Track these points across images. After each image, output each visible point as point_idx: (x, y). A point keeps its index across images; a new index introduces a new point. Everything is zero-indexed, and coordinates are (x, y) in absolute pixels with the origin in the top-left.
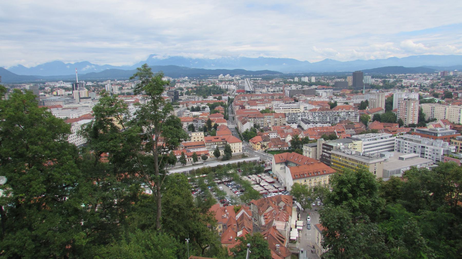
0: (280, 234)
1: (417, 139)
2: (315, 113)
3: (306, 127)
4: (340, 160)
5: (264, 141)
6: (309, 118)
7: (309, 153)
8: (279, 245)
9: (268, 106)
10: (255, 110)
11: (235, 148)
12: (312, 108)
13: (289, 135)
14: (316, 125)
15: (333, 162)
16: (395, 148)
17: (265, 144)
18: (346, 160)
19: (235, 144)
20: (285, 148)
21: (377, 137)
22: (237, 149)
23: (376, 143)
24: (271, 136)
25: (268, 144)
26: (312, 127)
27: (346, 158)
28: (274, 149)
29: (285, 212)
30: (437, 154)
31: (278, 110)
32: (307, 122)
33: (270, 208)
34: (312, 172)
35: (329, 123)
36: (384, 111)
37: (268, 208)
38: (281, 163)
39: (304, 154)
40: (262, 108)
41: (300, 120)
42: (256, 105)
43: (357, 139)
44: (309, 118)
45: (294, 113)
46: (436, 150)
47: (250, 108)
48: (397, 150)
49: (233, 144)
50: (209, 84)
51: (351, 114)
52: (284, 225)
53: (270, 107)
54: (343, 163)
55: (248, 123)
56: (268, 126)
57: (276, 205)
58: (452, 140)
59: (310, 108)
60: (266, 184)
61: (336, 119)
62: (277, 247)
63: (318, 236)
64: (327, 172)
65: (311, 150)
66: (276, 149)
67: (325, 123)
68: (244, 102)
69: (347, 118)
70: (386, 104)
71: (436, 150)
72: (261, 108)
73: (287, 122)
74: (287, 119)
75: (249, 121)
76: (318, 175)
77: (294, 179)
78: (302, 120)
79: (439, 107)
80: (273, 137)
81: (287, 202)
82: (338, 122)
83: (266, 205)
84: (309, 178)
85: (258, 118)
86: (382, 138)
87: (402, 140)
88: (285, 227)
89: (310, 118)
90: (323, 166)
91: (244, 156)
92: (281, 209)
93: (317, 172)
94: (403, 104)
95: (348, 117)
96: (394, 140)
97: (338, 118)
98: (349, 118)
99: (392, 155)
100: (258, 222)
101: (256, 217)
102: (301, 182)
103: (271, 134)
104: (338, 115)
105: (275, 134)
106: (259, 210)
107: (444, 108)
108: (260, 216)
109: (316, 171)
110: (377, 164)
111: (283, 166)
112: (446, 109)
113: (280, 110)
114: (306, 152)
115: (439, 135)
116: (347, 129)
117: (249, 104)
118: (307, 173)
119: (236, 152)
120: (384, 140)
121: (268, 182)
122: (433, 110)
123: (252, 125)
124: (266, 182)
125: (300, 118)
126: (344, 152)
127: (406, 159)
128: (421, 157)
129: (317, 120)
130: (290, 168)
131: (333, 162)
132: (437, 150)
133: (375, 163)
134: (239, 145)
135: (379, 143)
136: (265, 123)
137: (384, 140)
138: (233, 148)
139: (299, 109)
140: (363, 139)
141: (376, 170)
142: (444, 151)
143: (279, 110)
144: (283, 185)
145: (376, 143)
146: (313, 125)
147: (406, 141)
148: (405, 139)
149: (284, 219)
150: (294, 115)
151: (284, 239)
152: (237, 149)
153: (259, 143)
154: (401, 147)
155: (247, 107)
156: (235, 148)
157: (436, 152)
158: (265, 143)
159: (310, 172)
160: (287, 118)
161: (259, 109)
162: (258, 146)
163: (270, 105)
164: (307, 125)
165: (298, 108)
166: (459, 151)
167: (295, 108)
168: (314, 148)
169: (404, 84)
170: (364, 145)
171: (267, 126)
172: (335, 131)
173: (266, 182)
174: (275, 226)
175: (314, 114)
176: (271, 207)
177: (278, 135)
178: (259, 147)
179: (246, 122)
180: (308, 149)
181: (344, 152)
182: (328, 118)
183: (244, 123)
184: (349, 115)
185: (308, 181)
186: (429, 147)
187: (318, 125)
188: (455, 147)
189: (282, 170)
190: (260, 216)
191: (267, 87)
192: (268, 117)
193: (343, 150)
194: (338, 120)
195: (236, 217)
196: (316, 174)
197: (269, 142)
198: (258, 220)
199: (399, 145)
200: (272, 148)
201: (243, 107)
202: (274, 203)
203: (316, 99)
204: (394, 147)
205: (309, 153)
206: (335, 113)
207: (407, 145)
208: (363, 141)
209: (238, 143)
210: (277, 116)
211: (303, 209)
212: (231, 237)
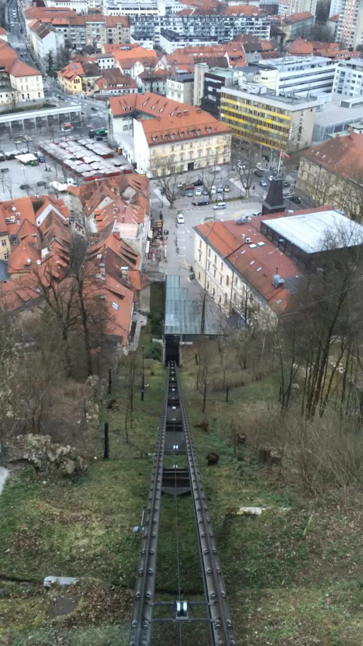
0: (128, 246)
2: (188, 17)
3: (169, 46)
4: (237, 107)
5: (89, 74)
6: (175, 29)
7: (179, 96)
8: (126, 268)
9: (94, 6)
10: (68, 10)
11: (27, 88)
12: (181, 9)
13: (138, 63)
14: (190, 43)
15: (224, 112)
16: (334, 87)
17: (91, 80)
18: (248, 107)
19: (26, 80)
21: (304, 63)
22: (33, 91)
23: (302, 76)
24: (101, 64)
25: (96, 81)
26: (183, 47)
27: (248, 102)
28: (110, 91)
29: (135, 206)
32: (173, 37)
33: (107, 201)
34: (185, 130)
35: (215, 39)
36: (314, 20)
37: (101, 200)
38: (124, 116)
39: (169, 96)
41: (157, 33)
43: (269, 68)
44: (175, 29)
45: (146, 17)
48: (337, 89)
49: (24, 79)
51: (256, 22)
52: (136, 229)
53: (98, 9)
54: (243, 114)
55: (52, 34)
56: (95, 44)
57: (118, 194)
59: (179, 10)
60: (97, 158)
61: (227, 33)
62: (124, 272)
63: (201, 247)
64: (214, 131)
65: (182, 89)
66: (114, 91)
67: (206, 40)
73: (133, 36)
74: (132, 30)
75: (55, 31)
76: (196, 137)
77: (150, 145)
78: (164, 33)
80: (106, 67)
81: (140, 188)
82: (231, 39)
83: (97, 194)
84: (180, 143)
85: (73, 26)
86: (313, 66)
88: (138, 233)
89: (180, 30)
90: (206, 118)
91: (47, 106)
92: (128, 202)
93: (194, 131)
95: (251, 28)
96: (333, 70)
97: (232, 30)
98: (252, 30)
99: (330, 99)
100: (84, 229)
101: (79, 220)
102: (165, 151)
103: (101, 60)
104: (232, 25)
105: (110, 59)
106: (84, 204)
108: (88, 216)
109: (192, 128)
110: (305, 112)
111: (127, 122)
114: (173, 94)
116: (247, 52)
118: (176, 133)
119: (31, 99)
120: (317, 69)
121: (100, 155)
123: (62, 40)
124: (97, 154)
125: (158, 29)
126: (245, 90)
127: (353, 105)
129: (192, 34)
130: (143, 121)
131: (224, 112)
134: (35, 82)
135: (307, 75)
137: (317, 69)
138: (25, 88)
139: (155, 12)
140: (279, 67)
141: (303, 126)
144: (129, 160)
145: (302, 76)
146: (185, 43)
147: (354, 72)
148: (354, 67)
149: (135, 219)
150: (146, 21)
151: (136, 256)
152: (33, 91)
153: (78, 78)
154: (345, 83)
156: (27, 88)
158: (91, 78)
159: (182, 130)
160: (132, 27)
161: (75, 10)
162: (76, 85)
164: (173, 43)
167: (148, 9)
168: (188, 84)
170: (281, 80)
172: (226, 55)
173: (97, 154)
174: (118, 233)
175: (186, 20)
176: (107, 198)
178: (79, 86)
179: (49, 32)
180: (176, 88)
181: (245, 90)
182: (213, 30)
183: (42, 34)
184: (252, 24)
185: (177, 149)
187: (195, 43)
189: (127, 132)
190: (88, 216)
192: (93, 25)
194: (232, 34)
195: (38, 220)
196: (194, 134)
197: (97, 77)
198: (84, 225)
199: (342, 81)
200: (105, 90)
202: (113, 190)
204: (331, 85)
205: (179, 96)
206: (226, 20)
207: (357, 79)
208: (280, 71)
209: (34, 78)
211: (169, 204)
212: (29, 261)
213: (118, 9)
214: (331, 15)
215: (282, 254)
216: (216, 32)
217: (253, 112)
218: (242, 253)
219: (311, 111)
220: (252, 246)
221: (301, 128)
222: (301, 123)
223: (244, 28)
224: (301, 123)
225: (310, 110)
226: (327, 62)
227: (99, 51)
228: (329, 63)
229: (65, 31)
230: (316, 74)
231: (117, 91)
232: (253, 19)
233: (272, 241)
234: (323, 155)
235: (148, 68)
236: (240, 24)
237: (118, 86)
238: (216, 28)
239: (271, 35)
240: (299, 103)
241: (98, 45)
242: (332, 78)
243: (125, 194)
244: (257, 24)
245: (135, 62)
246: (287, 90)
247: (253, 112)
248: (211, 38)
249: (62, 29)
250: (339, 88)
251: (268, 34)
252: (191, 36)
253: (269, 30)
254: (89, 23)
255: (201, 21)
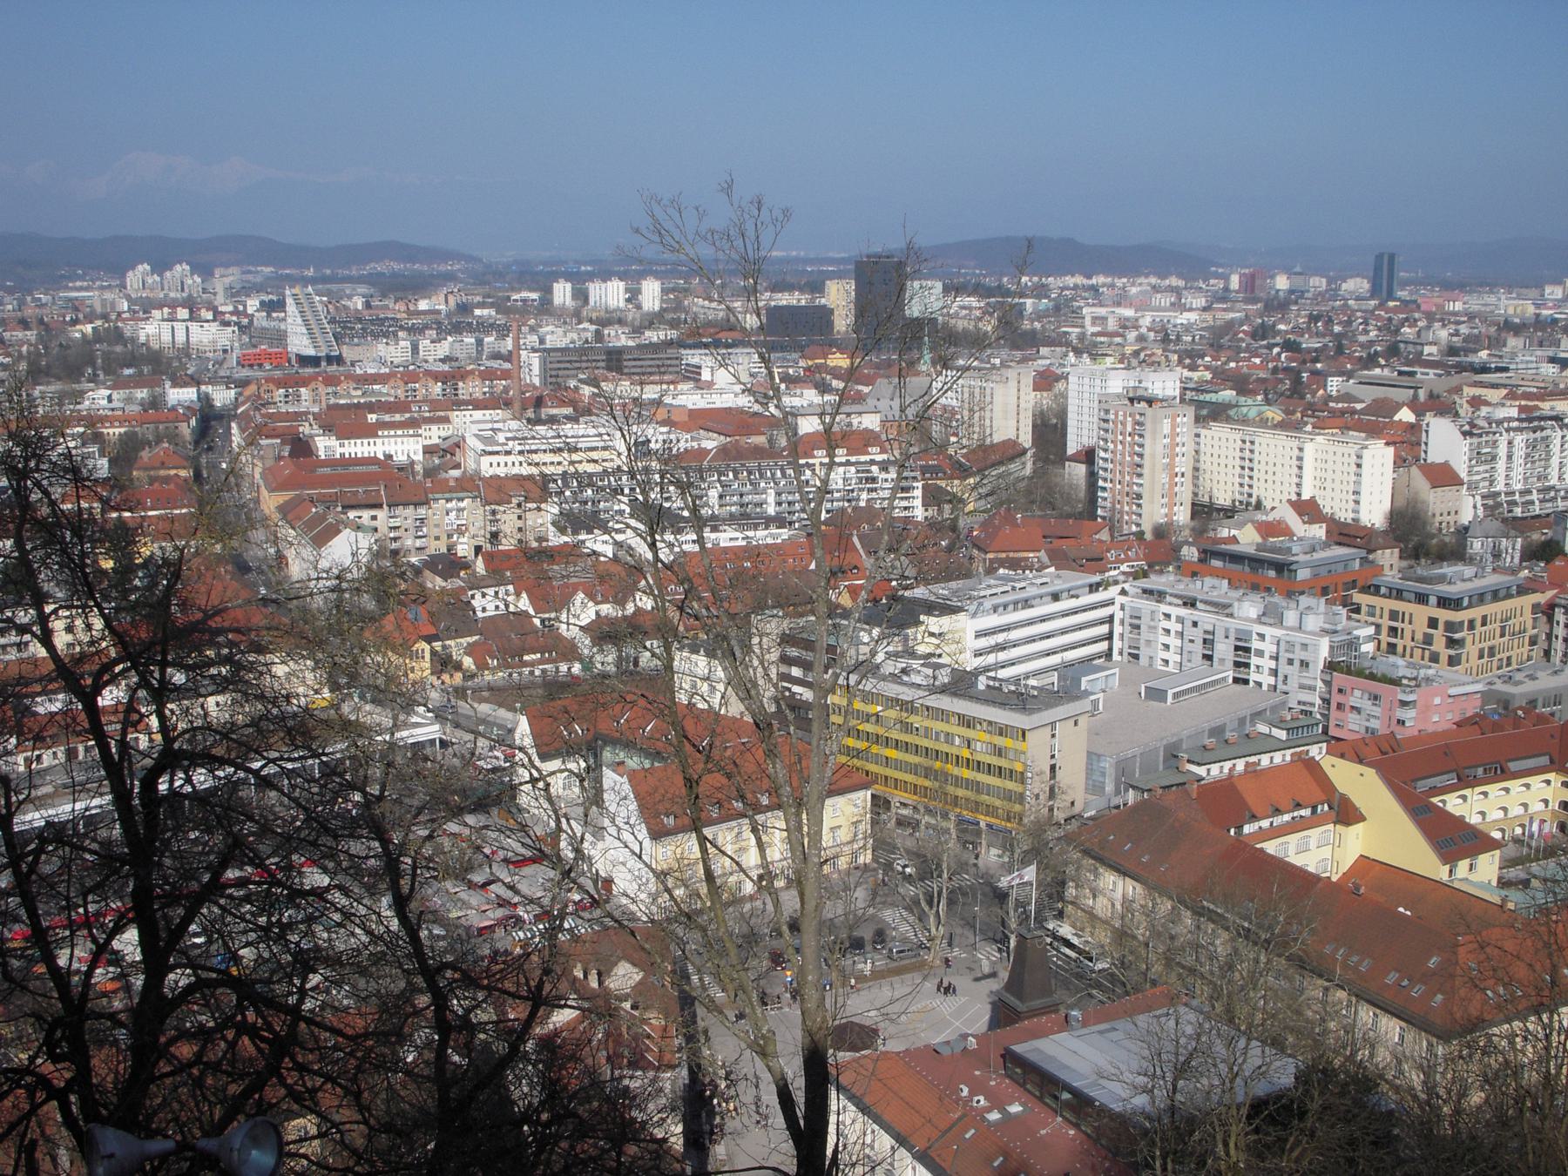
1: (1214, 596)
2: (700, 471)
9: (435, 441)
10: (373, 460)
20: (564, 668)
21: (1032, 591)
23: (1030, 622)
30: (1304, 664)
31: (495, 459)
35: (780, 521)
40: (406, 447)
42: (370, 432)
46: (1298, 647)
47: (340, 450)
50: (75, 322)
51: (883, 475)
57: (594, 984)
58: (1358, 597)
68: (298, 416)
69: (864, 496)
70: (1034, 426)
71: (1298, 647)
72: (399, 447)
79: (1272, 442)
86: (1056, 597)
87: (1146, 605)
94: (1124, 424)
95: (870, 490)
96: (1111, 602)
98: (874, 495)
107: (1295, 443)
112: (1301, 449)
113: (509, 459)
115: (1303, 574)
117: (328, 429)
122: (1247, 454)
127: (1176, 695)
128: (1236, 680)
132: (1305, 646)
133: (1053, 724)
136: (436, 532)
139: (606, 455)
142: (1331, 648)
143: (502, 459)
145: (1030, 622)
148: (1159, 596)
153: (423, 645)
155: (326, 445)
157: (1299, 655)
163: (443, 434)
165: (605, 449)
166: (1384, 646)
169: (1093, 324)
170: (980, 634)
171: (444, 550)
177: (518, 594)
179: (339, 532)
182: (771, 498)
184: (874, 480)
186: (1268, 631)
188: (1371, 630)
191: (412, 330)
193: (890, 668)
197: (471, 639)
201: (302, 448)
202: (579, 974)
203: (688, 398)
208: (974, 615)
210: (495, 492)
213: (508, 453)
214: (1072, 448)
215: (1072, 1132)
216: (779, 504)
217: (922, 732)
218: (967, 1136)
219: (1076, 723)
220: (994, 1116)
221: (1053, 768)
222: (1053, 757)
223: (853, 491)
224: (1053, 757)
225: (1072, 722)
226: (1091, 586)
227: (465, 565)
228: (1094, 588)
229: (374, 518)
230: (1065, 614)
231: (526, 670)
232: (875, 468)
233: (1041, 1099)
234: (1130, 849)
235: (607, 609)
236: (840, 482)
237: (526, 658)
238: (779, 494)
239: (926, 505)
240: (1039, 710)
241: (459, 547)
242: (1110, 620)
243: (612, 984)
244: (886, 480)
245: (574, 593)
246: (1002, 674)
247: (922, 732)
248: (769, 521)
249: (366, 515)
250: (1130, 647)
251: (918, 503)
252: (714, 517)
253: (918, 493)
254: (437, 496)
255: (736, 477)
